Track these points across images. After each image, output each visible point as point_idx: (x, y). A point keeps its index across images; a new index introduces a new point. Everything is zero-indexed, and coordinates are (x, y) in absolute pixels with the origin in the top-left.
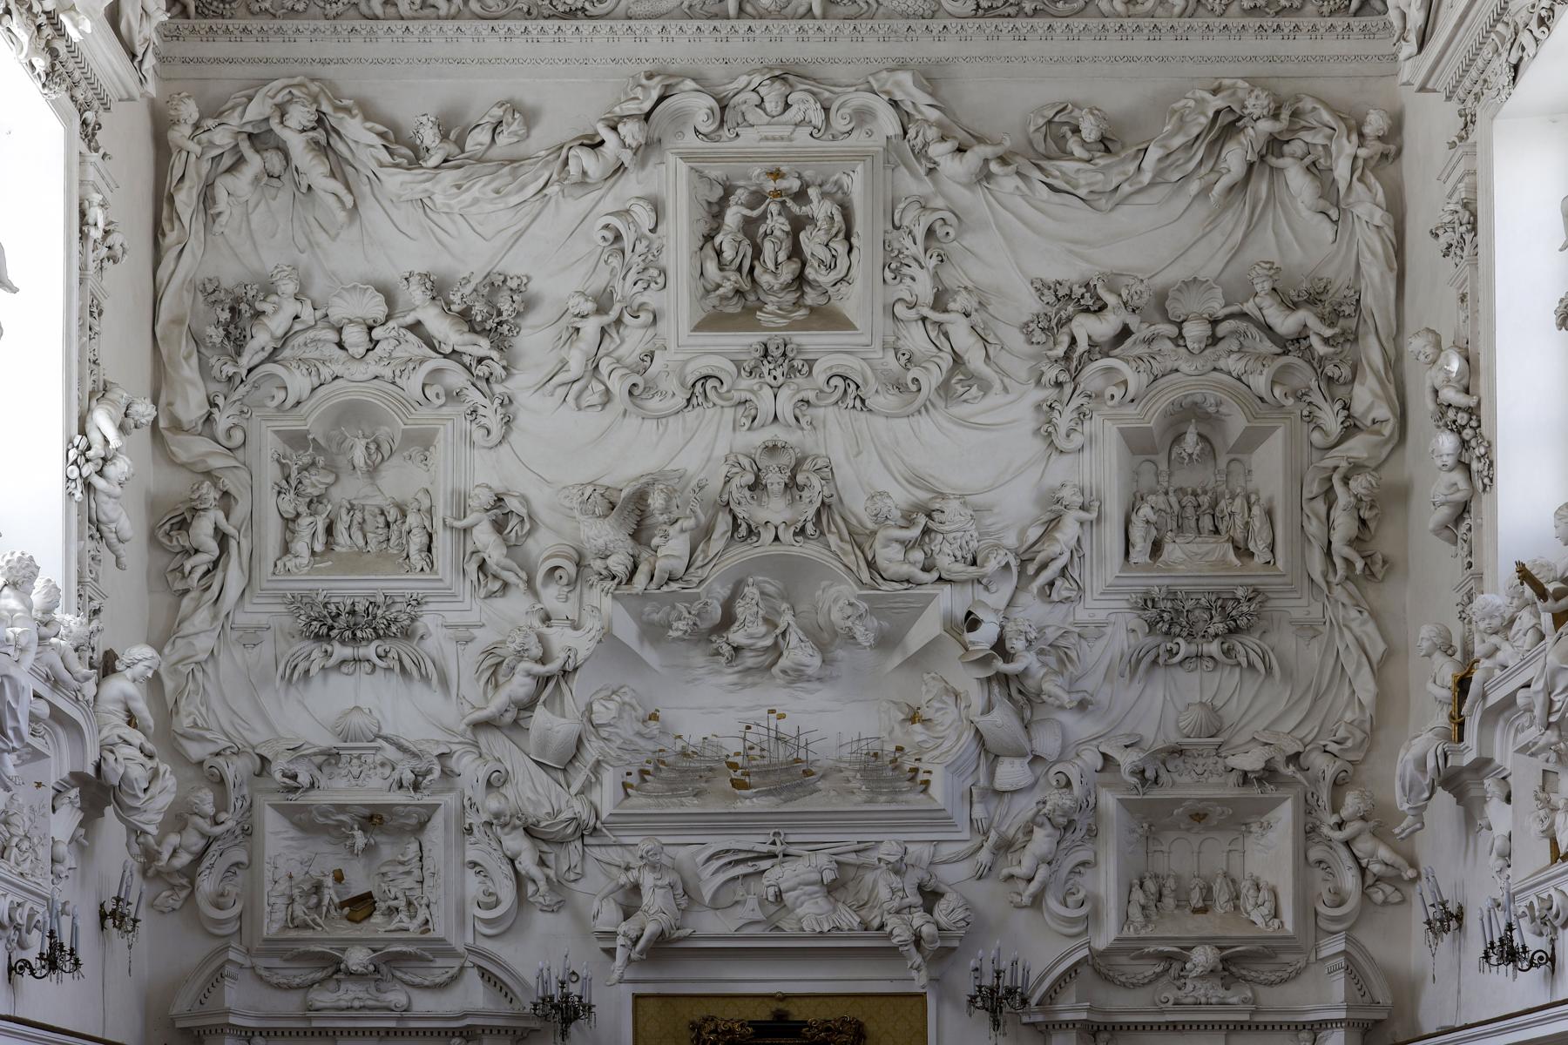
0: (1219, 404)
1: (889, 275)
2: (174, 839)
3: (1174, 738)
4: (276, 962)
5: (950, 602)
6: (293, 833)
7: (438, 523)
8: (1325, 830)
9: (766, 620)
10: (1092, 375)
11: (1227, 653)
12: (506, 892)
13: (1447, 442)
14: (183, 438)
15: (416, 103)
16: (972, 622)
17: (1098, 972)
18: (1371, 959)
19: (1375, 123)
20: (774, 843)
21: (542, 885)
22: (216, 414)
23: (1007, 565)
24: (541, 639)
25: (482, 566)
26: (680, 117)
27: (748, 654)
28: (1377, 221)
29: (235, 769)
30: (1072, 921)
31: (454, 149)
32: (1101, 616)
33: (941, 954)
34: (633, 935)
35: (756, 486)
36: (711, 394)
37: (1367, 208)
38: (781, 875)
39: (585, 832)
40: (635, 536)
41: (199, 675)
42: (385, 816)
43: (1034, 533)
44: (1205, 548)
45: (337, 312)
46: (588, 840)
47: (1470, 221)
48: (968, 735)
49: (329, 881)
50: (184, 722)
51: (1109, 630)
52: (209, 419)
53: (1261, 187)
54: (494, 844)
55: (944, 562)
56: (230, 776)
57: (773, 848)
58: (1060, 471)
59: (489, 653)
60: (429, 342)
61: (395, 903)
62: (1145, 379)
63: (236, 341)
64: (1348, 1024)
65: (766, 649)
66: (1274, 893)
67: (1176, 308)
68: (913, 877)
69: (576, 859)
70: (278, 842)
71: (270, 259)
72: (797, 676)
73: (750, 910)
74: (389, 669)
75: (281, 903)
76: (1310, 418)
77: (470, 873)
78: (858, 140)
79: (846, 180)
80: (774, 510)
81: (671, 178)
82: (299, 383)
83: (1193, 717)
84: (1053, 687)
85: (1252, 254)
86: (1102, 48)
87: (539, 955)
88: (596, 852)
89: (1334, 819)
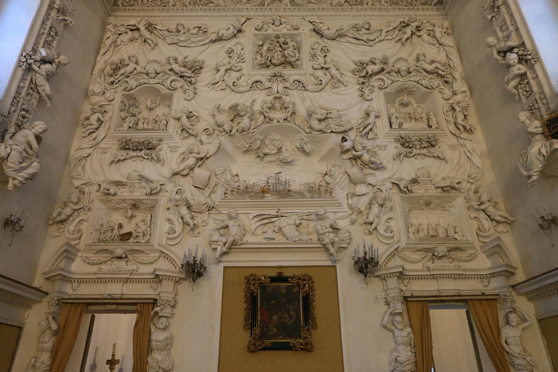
4: (91, 255)
20: (278, 212)
32: (385, 143)
36: (258, 86)
42: (140, 205)
46: (210, 212)
49: (116, 227)
51: (388, 148)
54: (177, 213)
57: (277, 214)
61: (138, 234)
62: (390, 82)
86: (366, 13)
88: (213, 216)
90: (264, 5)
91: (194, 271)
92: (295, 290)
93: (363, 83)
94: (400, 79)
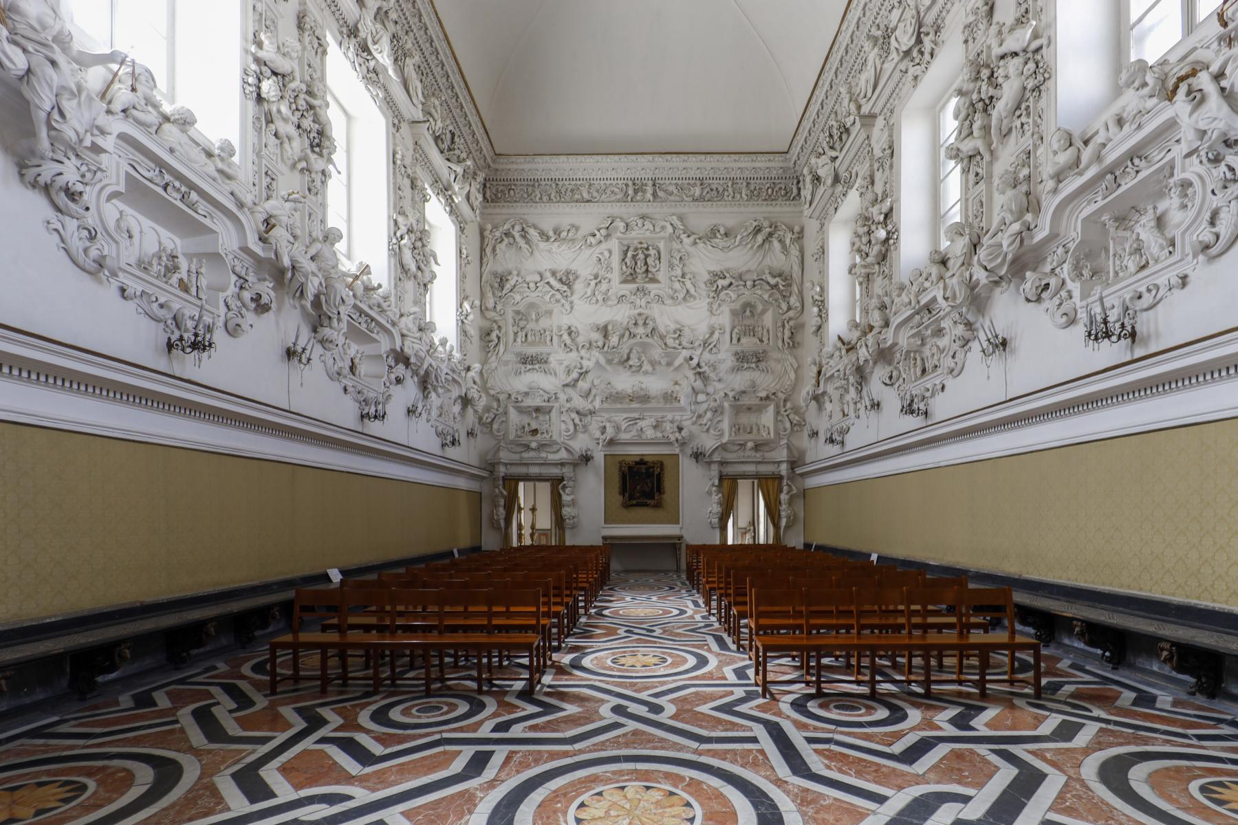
5: (686, 353)
12: (572, 428)
13: (816, 309)
15: (548, 225)
16: (691, 359)
19: (797, 229)
26: (616, 229)
29: (502, 397)
33: (683, 444)
35: (636, 324)
37: (794, 251)
38: (641, 424)
39: (592, 413)
45: (528, 279)
47: (823, 251)
50: (489, 385)
55: (684, 343)
58: (714, 320)
63: (502, 287)
64: (788, 462)
67: (744, 278)
70: (513, 415)
71: (510, 265)
73: (634, 433)
78: (662, 234)
80: (640, 330)
81: (614, 244)
82: (518, 297)
84: (712, 375)
85: (765, 263)
91: (586, 459)
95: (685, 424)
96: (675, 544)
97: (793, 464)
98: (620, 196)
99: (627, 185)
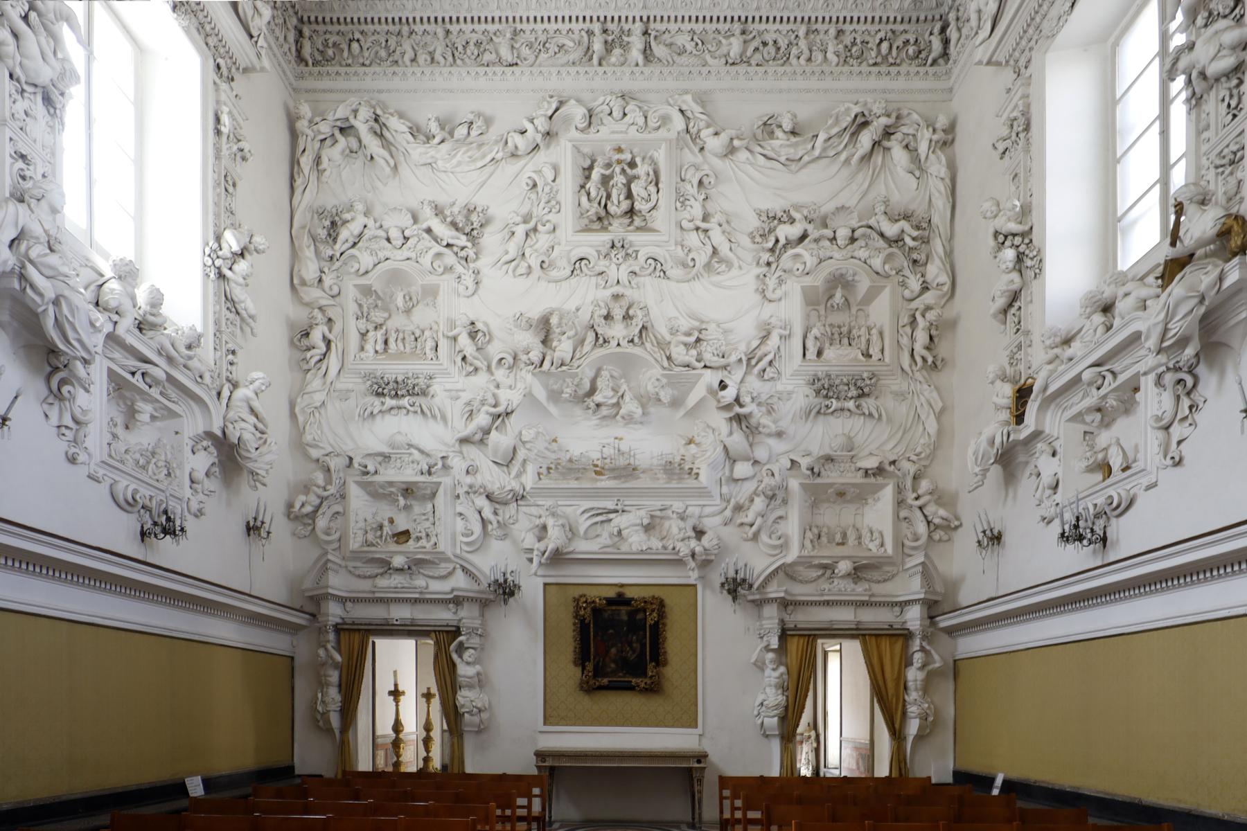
0: (854, 275)
1: (679, 205)
2: (302, 498)
3: (827, 451)
4: (359, 564)
6: (366, 497)
7: (440, 335)
8: (910, 501)
9: (613, 389)
10: (786, 260)
11: (858, 407)
12: (477, 528)
14: (306, 288)
15: (427, 113)
17: (787, 575)
18: (936, 568)
21: (495, 523)
22: (324, 277)
23: (740, 360)
24: (494, 395)
25: (464, 358)
26: (568, 120)
27: (603, 408)
28: (942, 175)
29: (334, 463)
30: (774, 547)
31: (447, 136)
32: (790, 388)
34: (542, 549)
35: (608, 317)
38: (619, 521)
39: (519, 498)
40: (545, 342)
41: (317, 414)
43: (755, 343)
44: (846, 352)
48: (720, 449)
49: (386, 523)
50: (308, 438)
52: (320, 280)
53: (878, 158)
56: (332, 468)
58: (769, 309)
59: (468, 404)
60: (436, 240)
62: (816, 261)
65: (614, 405)
66: (881, 534)
68: (690, 523)
69: (513, 512)
70: (358, 500)
72: (629, 420)
73: (605, 539)
74: (416, 412)
75: (360, 533)
76: (903, 285)
77: (459, 519)
79: (656, 155)
81: (563, 154)
82: (366, 260)
83: (841, 440)
87: (494, 560)
88: (524, 509)
89: (915, 495)
90: (591, 59)
92: (640, 616)
93: (769, 264)
94: (837, 255)
95: (708, 523)
96: (690, 770)
97: (933, 609)
98: (576, 55)
99: (590, 33)
